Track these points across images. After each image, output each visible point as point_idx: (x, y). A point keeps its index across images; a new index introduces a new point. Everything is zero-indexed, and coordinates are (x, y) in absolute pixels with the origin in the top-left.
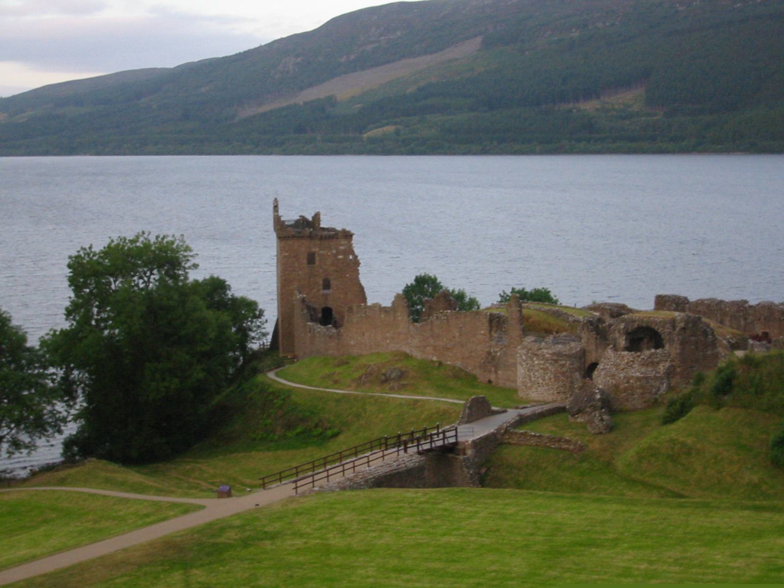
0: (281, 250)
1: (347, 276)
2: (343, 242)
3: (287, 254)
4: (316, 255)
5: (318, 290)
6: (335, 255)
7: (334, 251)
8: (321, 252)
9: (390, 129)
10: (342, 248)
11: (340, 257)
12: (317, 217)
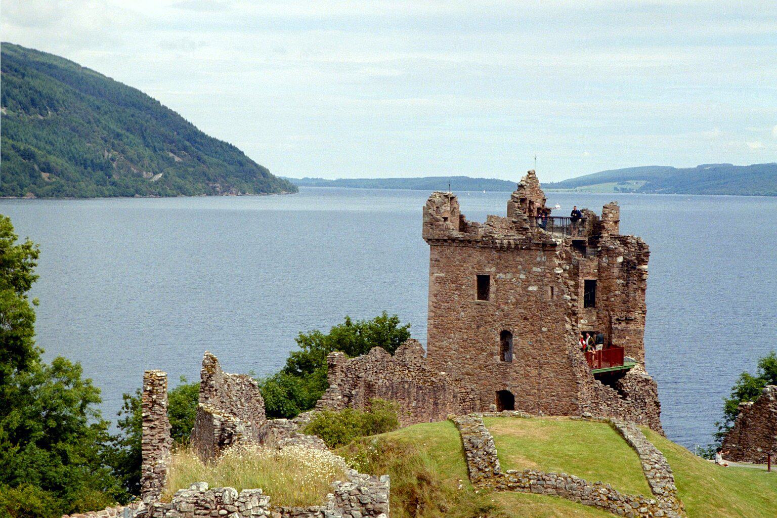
0: (435, 263)
1: (544, 329)
2: (541, 257)
3: (441, 275)
4: (492, 281)
5: (491, 354)
6: (526, 283)
7: (523, 277)
8: (501, 275)
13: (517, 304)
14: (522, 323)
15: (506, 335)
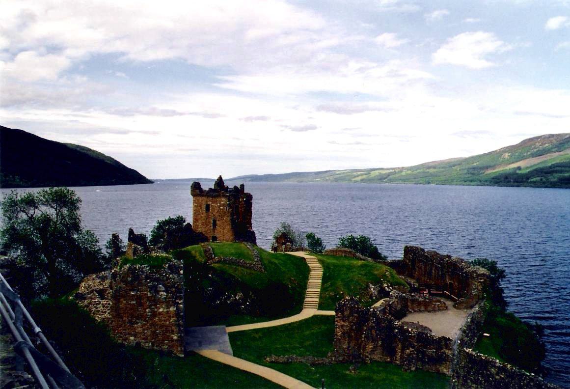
2: (223, 199)
5: (211, 226)
6: (219, 207)
7: (219, 205)
9: (538, 179)
10: (222, 202)
11: (222, 208)
12: (242, 186)
13: (217, 212)
14: (219, 217)
15: (215, 221)
